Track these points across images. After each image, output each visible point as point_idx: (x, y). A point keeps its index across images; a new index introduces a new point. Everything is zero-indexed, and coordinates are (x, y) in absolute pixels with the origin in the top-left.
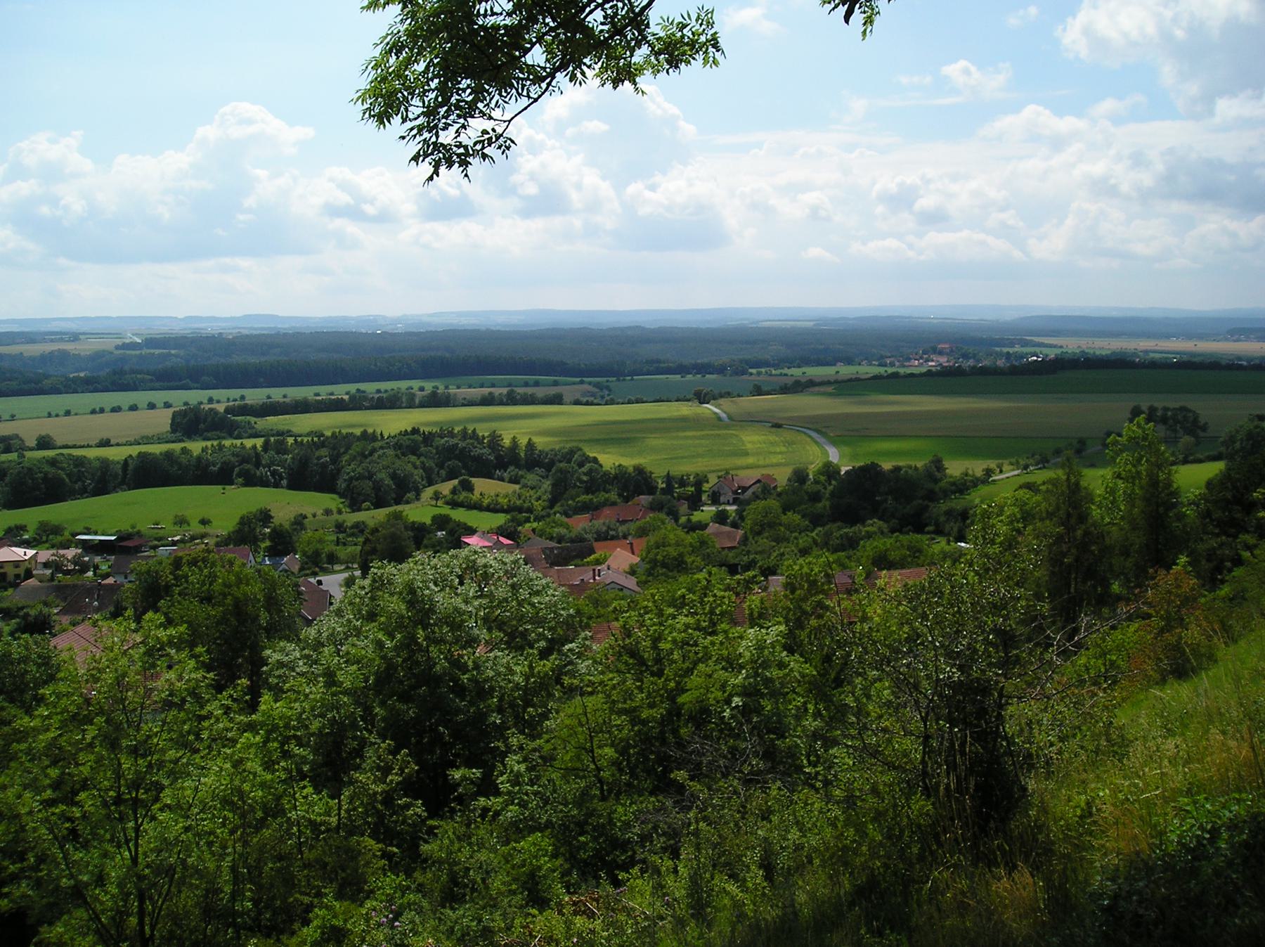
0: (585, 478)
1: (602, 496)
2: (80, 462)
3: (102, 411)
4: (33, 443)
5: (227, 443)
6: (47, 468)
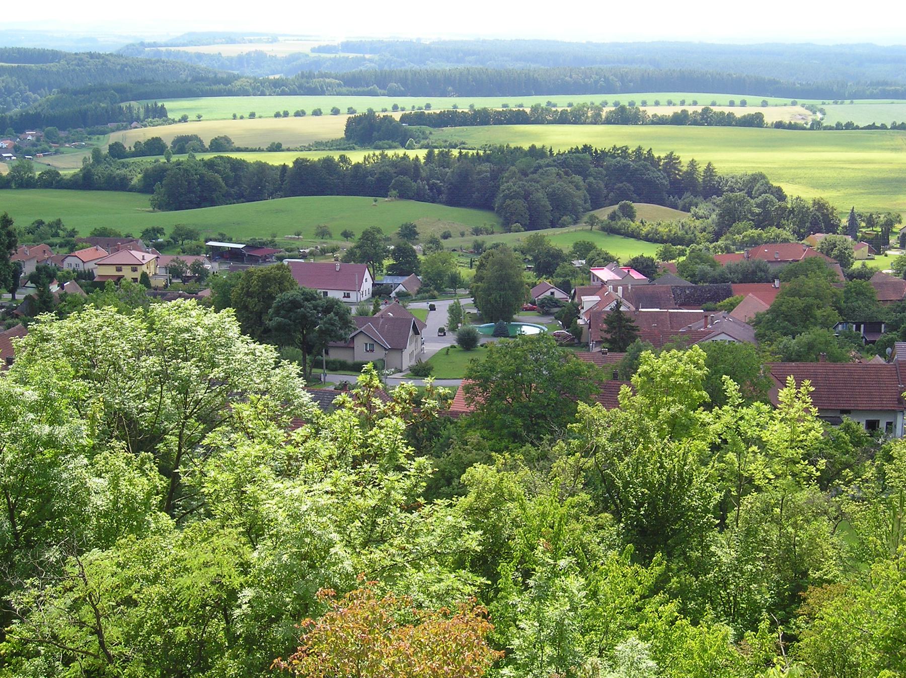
0: (757, 210)
1: (773, 231)
2: (238, 166)
3: (286, 114)
4: (207, 144)
5: (390, 153)
6: (204, 171)
